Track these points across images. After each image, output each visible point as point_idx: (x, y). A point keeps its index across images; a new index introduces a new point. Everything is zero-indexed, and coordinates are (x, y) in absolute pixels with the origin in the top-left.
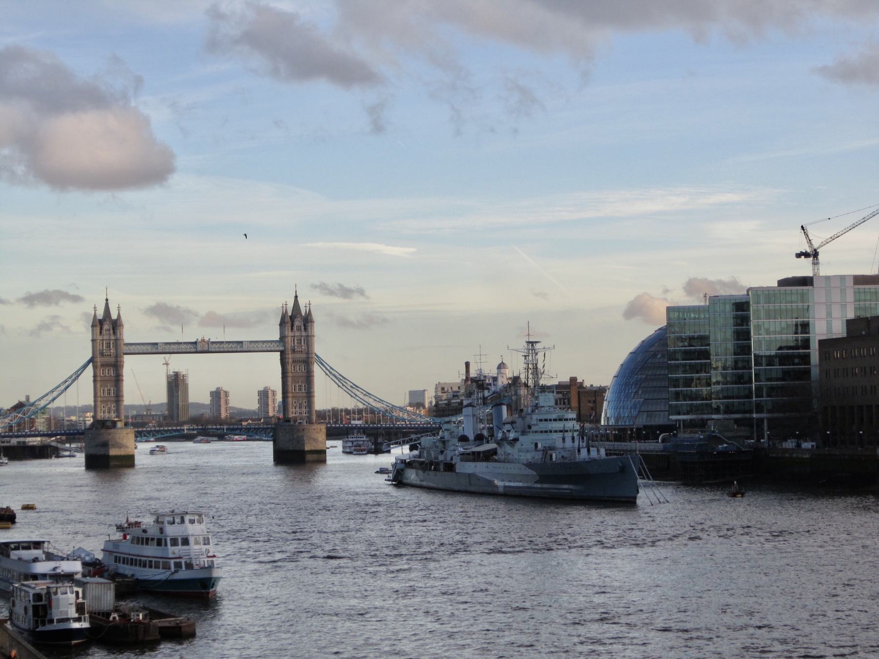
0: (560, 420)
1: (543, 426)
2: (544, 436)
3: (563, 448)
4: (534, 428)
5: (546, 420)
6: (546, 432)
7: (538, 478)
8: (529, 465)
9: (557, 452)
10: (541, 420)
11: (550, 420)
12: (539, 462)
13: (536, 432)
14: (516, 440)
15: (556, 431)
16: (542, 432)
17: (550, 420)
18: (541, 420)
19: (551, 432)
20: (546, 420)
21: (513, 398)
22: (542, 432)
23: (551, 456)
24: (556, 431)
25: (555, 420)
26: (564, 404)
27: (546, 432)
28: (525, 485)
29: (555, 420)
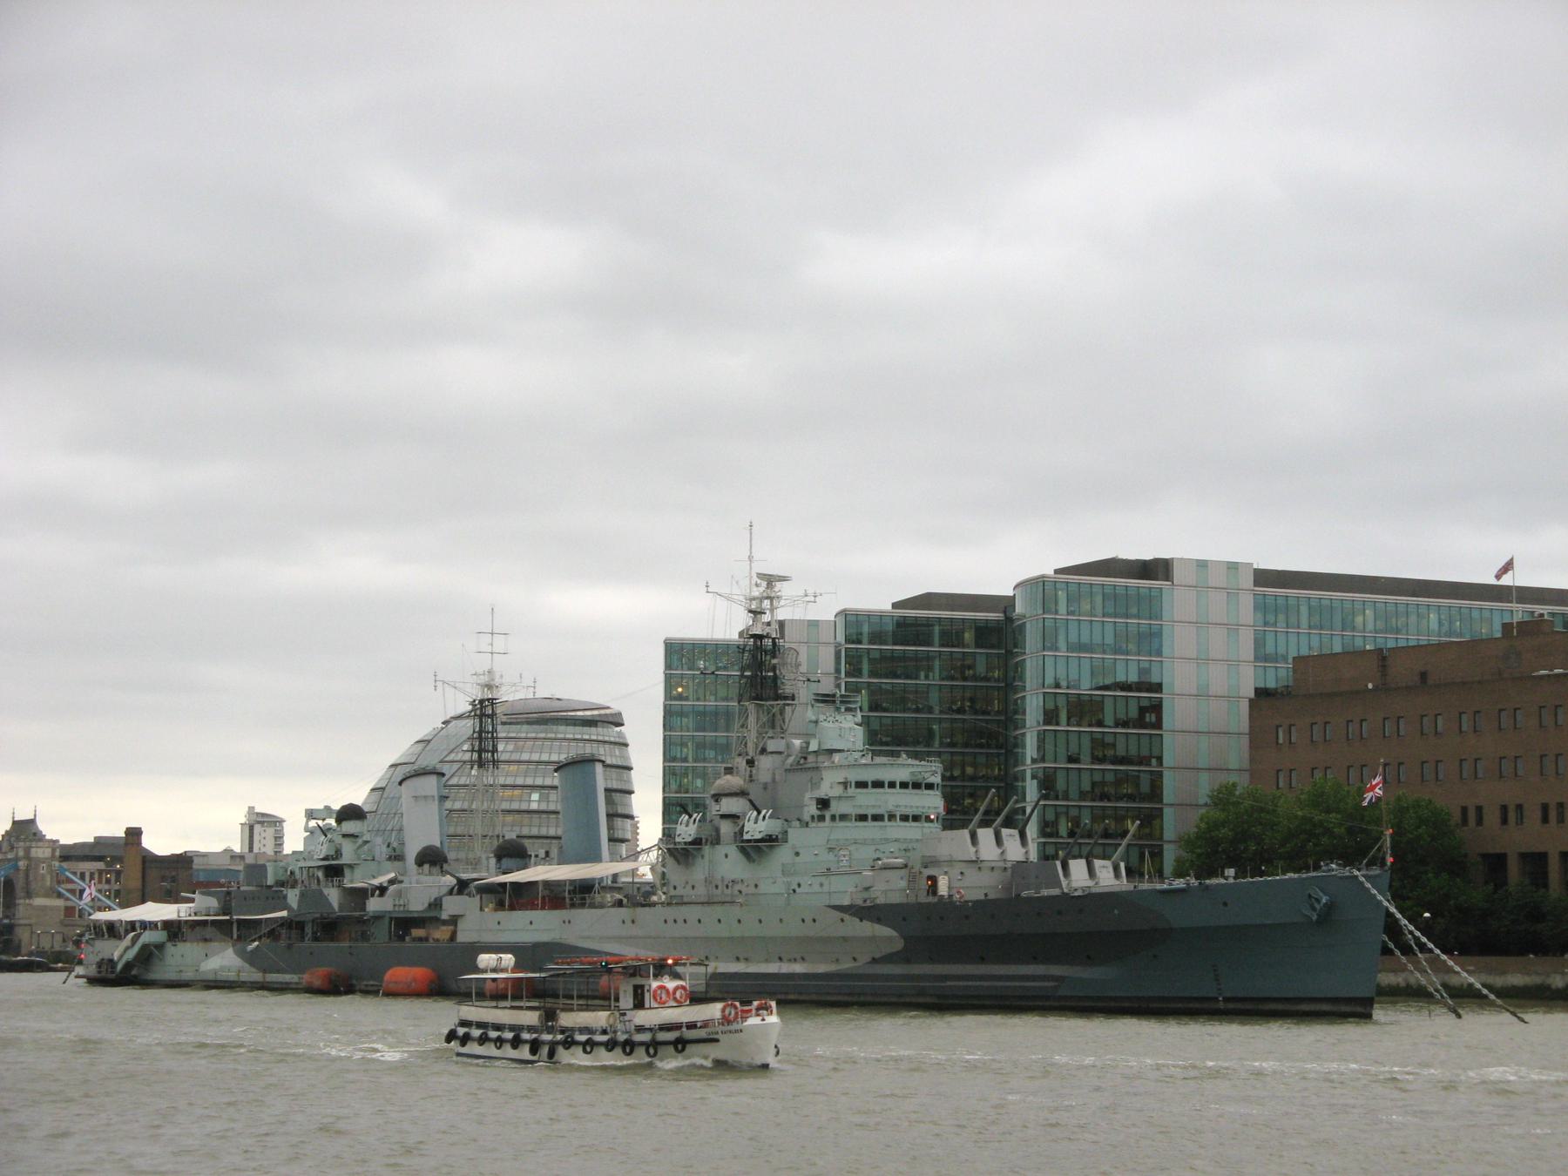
0: (916, 786)
1: (869, 801)
2: (870, 830)
3: (976, 863)
4: (836, 808)
5: (878, 784)
6: (877, 818)
7: (899, 945)
8: (866, 912)
9: (955, 872)
10: (861, 785)
11: (892, 785)
12: (896, 899)
13: (843, 817)
14: (770, 840)
15: (905, 818)
16: (863, 818)
17: (892, 785)
18: (861, 785)
19: (892, 817)
20: (878, 784)
21: (22, 864)
22: (863, 818)
23: (933, 879)
24: (905, 818)
25: (904, 785)
26: (108, 881)
27: (877, 818)
28: (822, 968)
29: (904, 785)
